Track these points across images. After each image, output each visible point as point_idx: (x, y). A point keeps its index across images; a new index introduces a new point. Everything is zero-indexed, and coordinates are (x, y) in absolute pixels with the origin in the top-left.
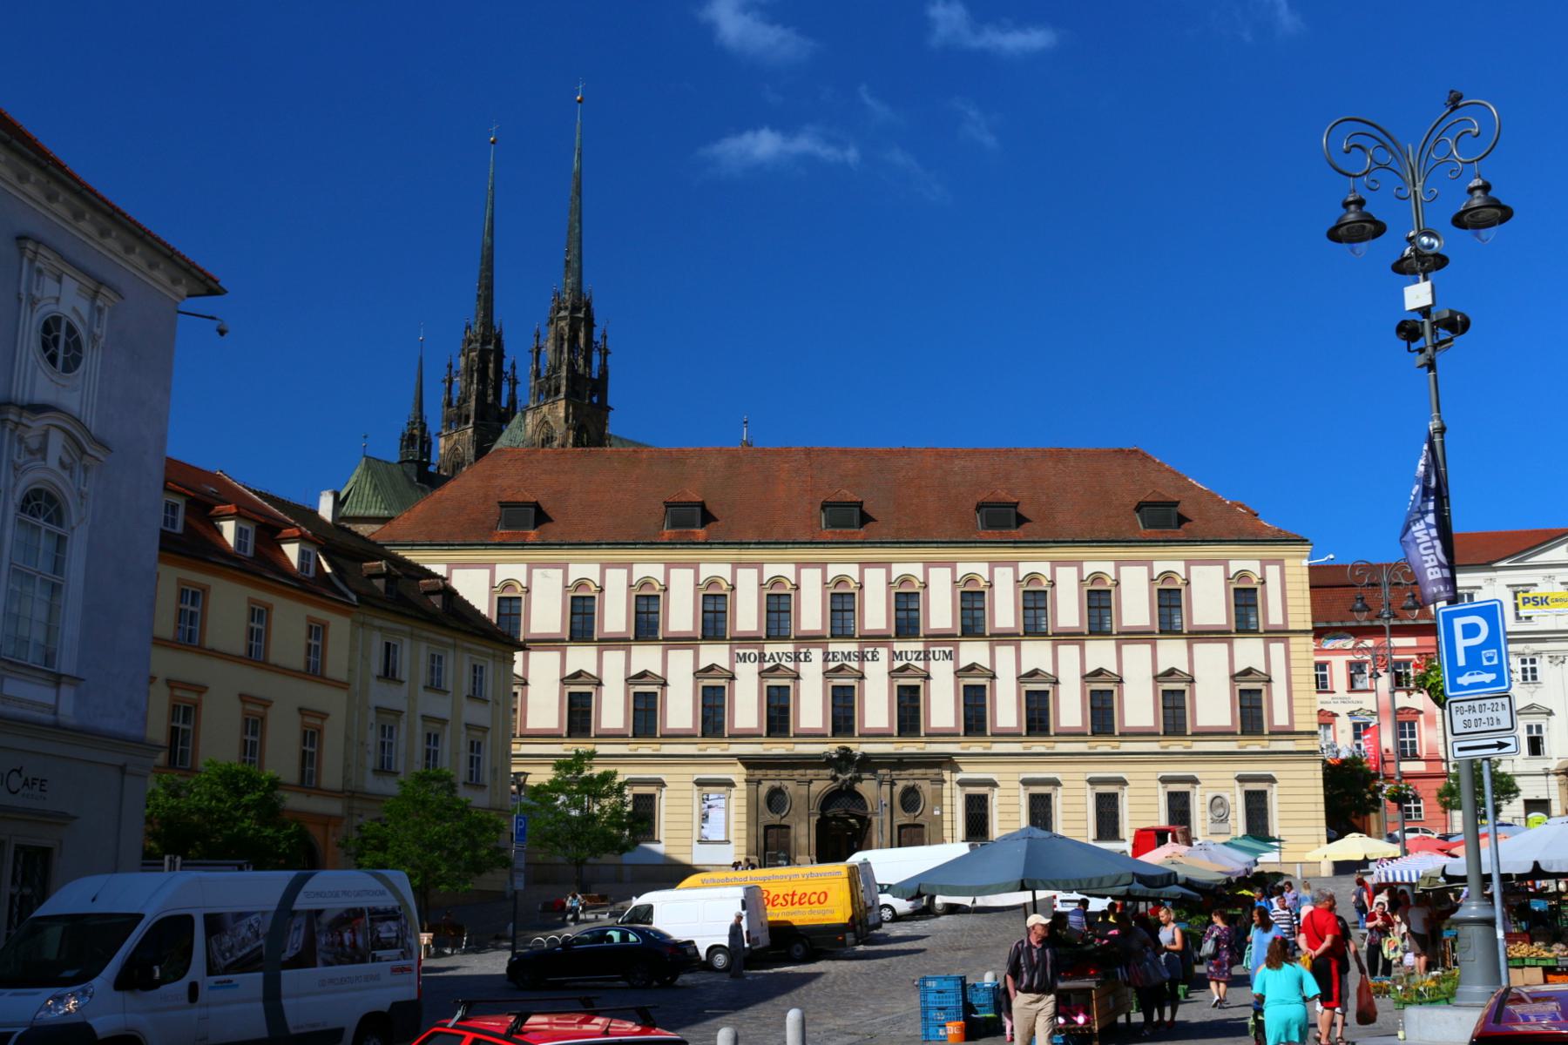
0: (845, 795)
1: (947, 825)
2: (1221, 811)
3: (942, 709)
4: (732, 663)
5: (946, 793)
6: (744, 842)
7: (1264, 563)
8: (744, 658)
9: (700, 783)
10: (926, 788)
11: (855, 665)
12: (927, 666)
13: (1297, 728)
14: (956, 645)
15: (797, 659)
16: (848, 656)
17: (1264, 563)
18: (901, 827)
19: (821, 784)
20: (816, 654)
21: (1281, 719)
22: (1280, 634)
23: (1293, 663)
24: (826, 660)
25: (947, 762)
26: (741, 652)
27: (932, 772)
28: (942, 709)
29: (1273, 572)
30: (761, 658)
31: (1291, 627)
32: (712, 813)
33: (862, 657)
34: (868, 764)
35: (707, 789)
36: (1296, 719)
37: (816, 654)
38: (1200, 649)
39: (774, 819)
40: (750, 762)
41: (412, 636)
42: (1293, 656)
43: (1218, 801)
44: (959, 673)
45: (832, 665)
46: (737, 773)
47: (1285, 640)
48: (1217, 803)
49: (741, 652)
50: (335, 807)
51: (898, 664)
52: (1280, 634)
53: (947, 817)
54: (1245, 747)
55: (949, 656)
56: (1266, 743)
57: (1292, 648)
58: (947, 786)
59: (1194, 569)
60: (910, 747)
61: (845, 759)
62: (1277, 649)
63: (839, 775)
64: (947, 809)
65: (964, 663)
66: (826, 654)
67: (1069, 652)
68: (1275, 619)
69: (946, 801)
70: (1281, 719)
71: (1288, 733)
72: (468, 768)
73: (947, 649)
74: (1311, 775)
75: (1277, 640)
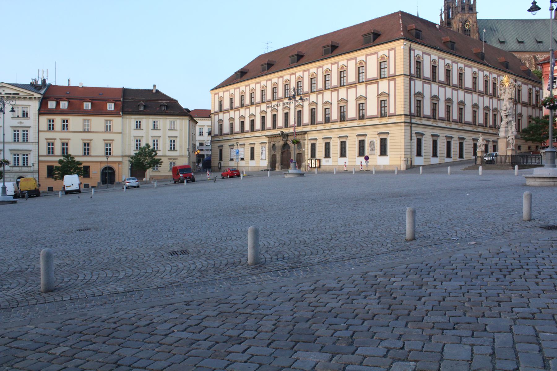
0: (286, 145)
1: (306, 153)
2: (373, 146)
3: (306, 118)
4: (266, 109)
5: (306, 143)
6: (268, 160)
7: (389, 50)
8: (268, 107)
9: (261, 143)
10: (302, 142)
11: (288, 106)
12: (303, 104)
13: (397, 114)
14: (309, 96)
15: (278, 106)
16: (287, 103)
17: (389, 50)
18: (297, 154)
19: (281, 143)
20: (281, 103)
21: (392, 111)
22: (392, 77)
23: (397, 88)
24: (283, 105)
25: (305, 133)
26: (268, 105)
27: (303, 136)
28: (306, 118)
29: (392, 53)
30: (272, 106)
31: (396, 74)
32: (264, 152)
33: (290, 104)
34: (287, 135)
35: (263, 145)
36: (397, 110)
37: (281, 103)
38: (369, 86)
39: (273, 153)
40: (269, 137)
41: (145, 118)
42: (397, 85)
43: (372, 143)
44: (311, 104)
45: (284, 106)
46: (266, 140)
47: (395, 80)
48: (372, 144)
49: (268, 105)
50: (120, 159)
51: (297, 104)
52: (392, 77)
53: (306, 151)
54: (381, 122)
55: (307, 100)
56: (387, 120)
57: (397, 82)
58: (306, 141)
59: (368, 57)
60: (299, 129)
61: (283, 135)
62: (392, 83)
63: (284, 140)
64: (306, 148)
65: (311, 101)
66: (283, 103)
67: (335, 94)
68: (392, 72)
69: (306, 146)
70: (392, 111)
71: (394, 115)
72: (170, 146)
73: (307, 98)
74: (399, 131)
75: (392, 80)
